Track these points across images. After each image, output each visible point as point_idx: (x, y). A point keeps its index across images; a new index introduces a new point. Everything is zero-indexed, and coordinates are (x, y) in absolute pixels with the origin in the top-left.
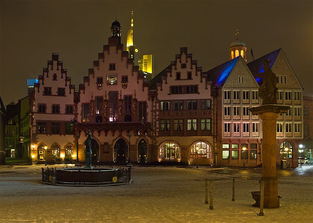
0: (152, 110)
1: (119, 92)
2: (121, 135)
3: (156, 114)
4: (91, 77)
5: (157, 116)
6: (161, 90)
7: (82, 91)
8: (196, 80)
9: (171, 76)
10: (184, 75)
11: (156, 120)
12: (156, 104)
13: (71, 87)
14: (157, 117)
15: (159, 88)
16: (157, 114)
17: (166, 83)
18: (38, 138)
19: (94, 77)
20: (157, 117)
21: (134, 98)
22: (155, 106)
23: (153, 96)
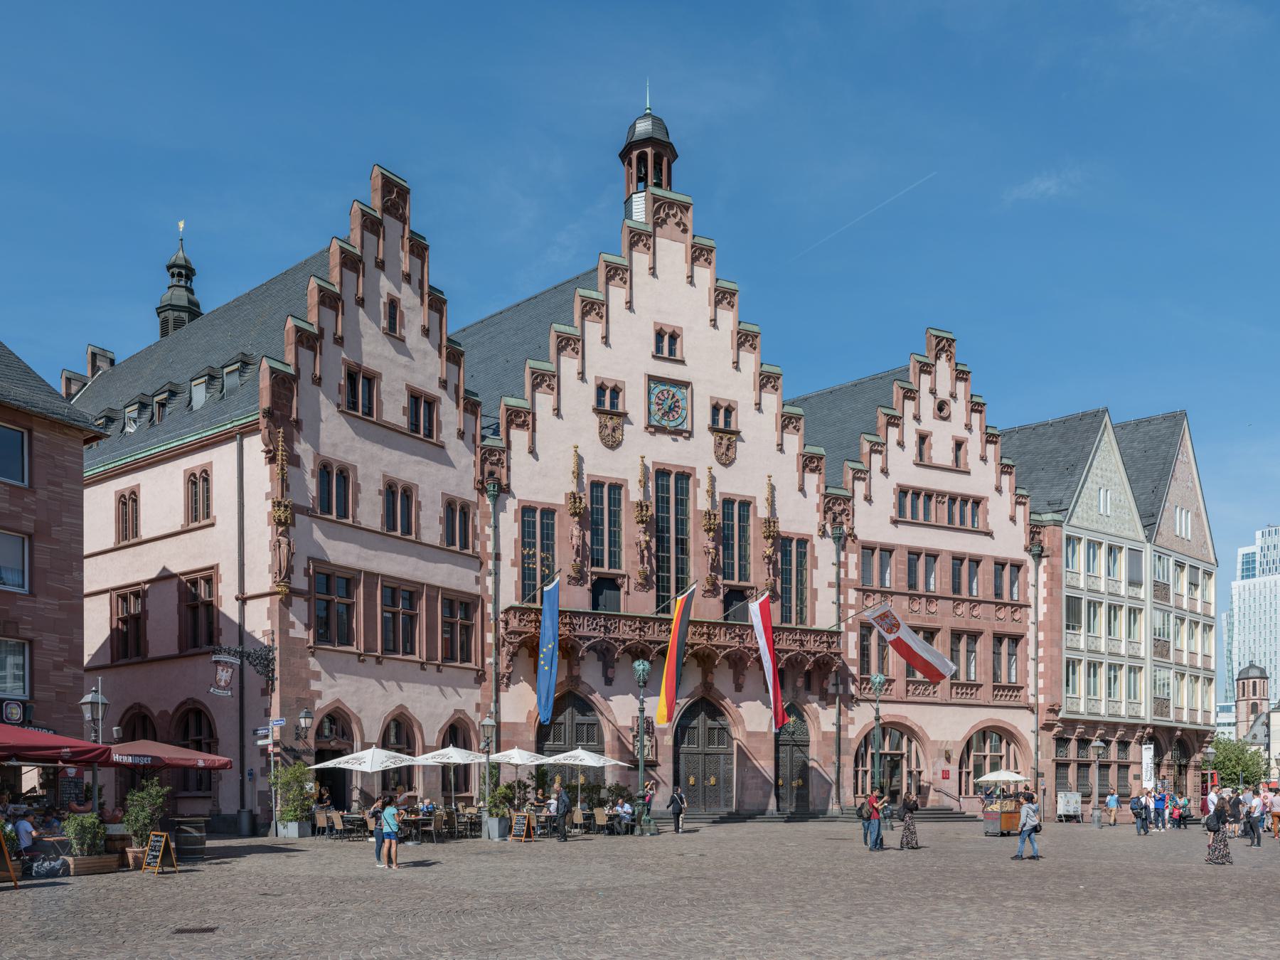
0: (834, 580)
1: (702, 476)
2: (707, 686)
3: (846, 599)
4: (569, 365)
5: (852, 607)
6: (868, 499)
7: (519, 438)
8: (982, 477)
9: (901, 444)
10: (941, 452)
11: (849, 628)
12: (846, 558)
13: (471, 406)
14: (851, 612)
15: (860, 487)
16: (852, 601)
17: (885, 471)
18: (317, 676)
19: (582, 376)
20: (851, 612)
21: (763, 512)
22: (846, 564)
23: (834, 520)
